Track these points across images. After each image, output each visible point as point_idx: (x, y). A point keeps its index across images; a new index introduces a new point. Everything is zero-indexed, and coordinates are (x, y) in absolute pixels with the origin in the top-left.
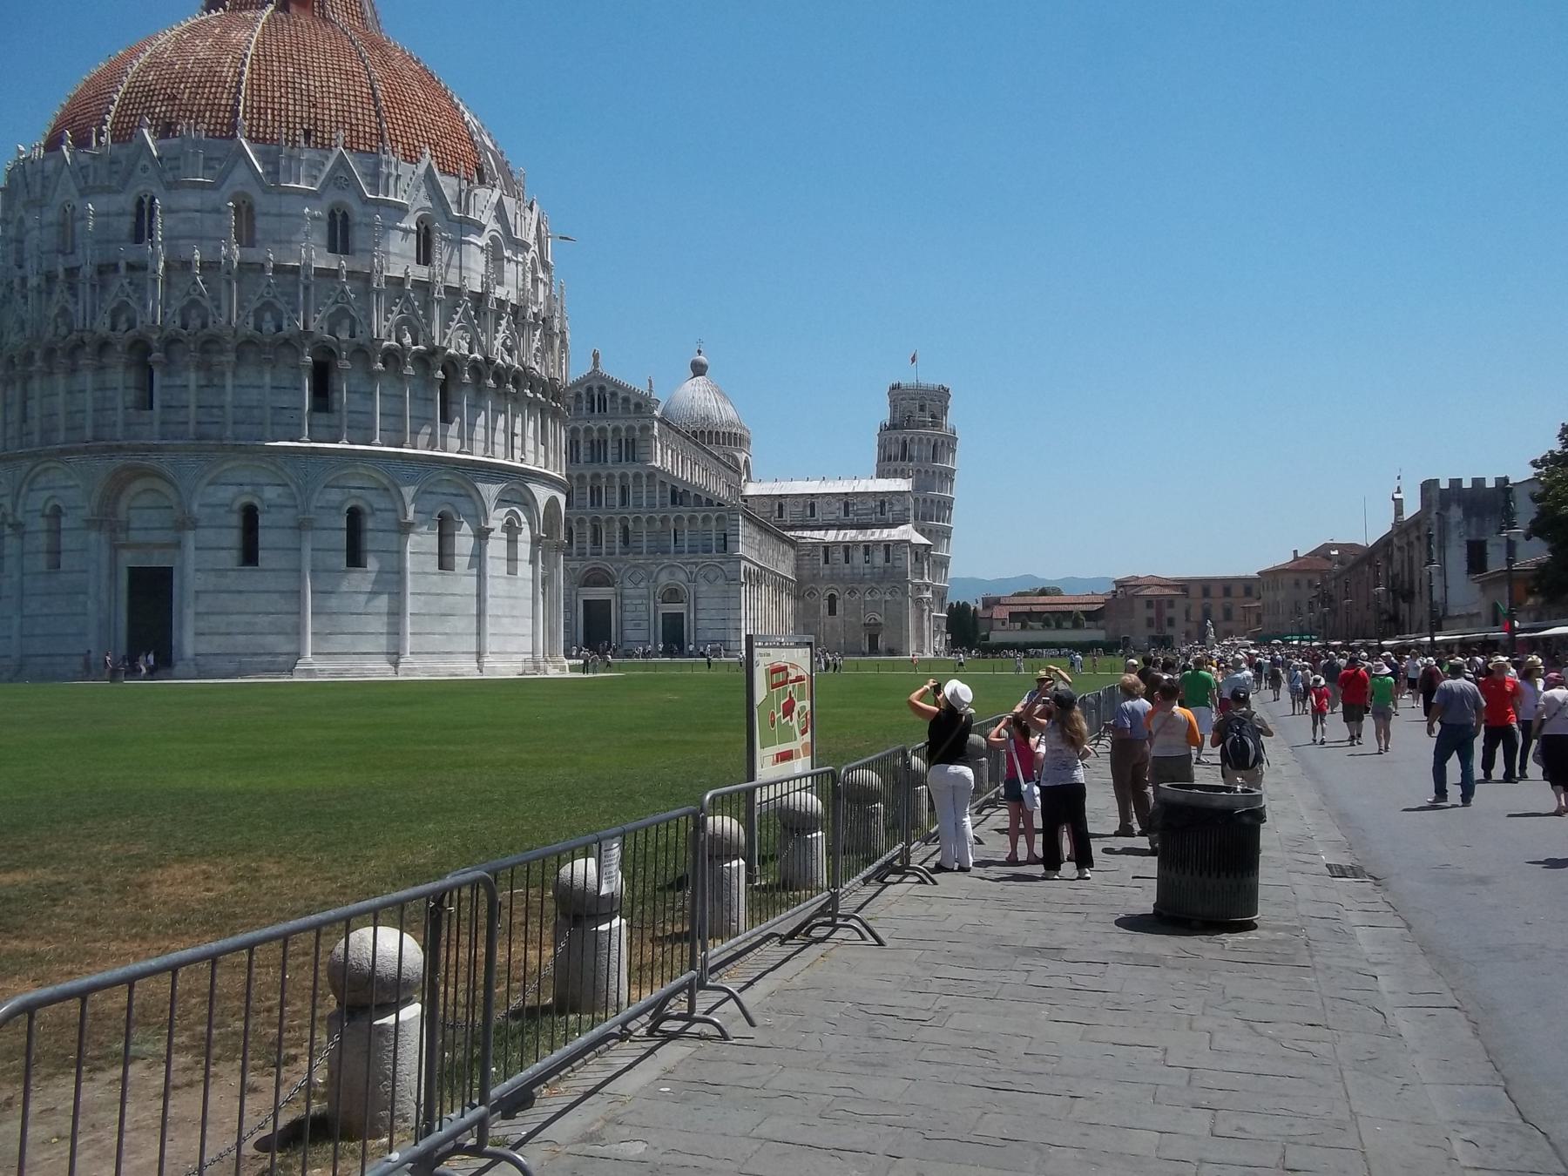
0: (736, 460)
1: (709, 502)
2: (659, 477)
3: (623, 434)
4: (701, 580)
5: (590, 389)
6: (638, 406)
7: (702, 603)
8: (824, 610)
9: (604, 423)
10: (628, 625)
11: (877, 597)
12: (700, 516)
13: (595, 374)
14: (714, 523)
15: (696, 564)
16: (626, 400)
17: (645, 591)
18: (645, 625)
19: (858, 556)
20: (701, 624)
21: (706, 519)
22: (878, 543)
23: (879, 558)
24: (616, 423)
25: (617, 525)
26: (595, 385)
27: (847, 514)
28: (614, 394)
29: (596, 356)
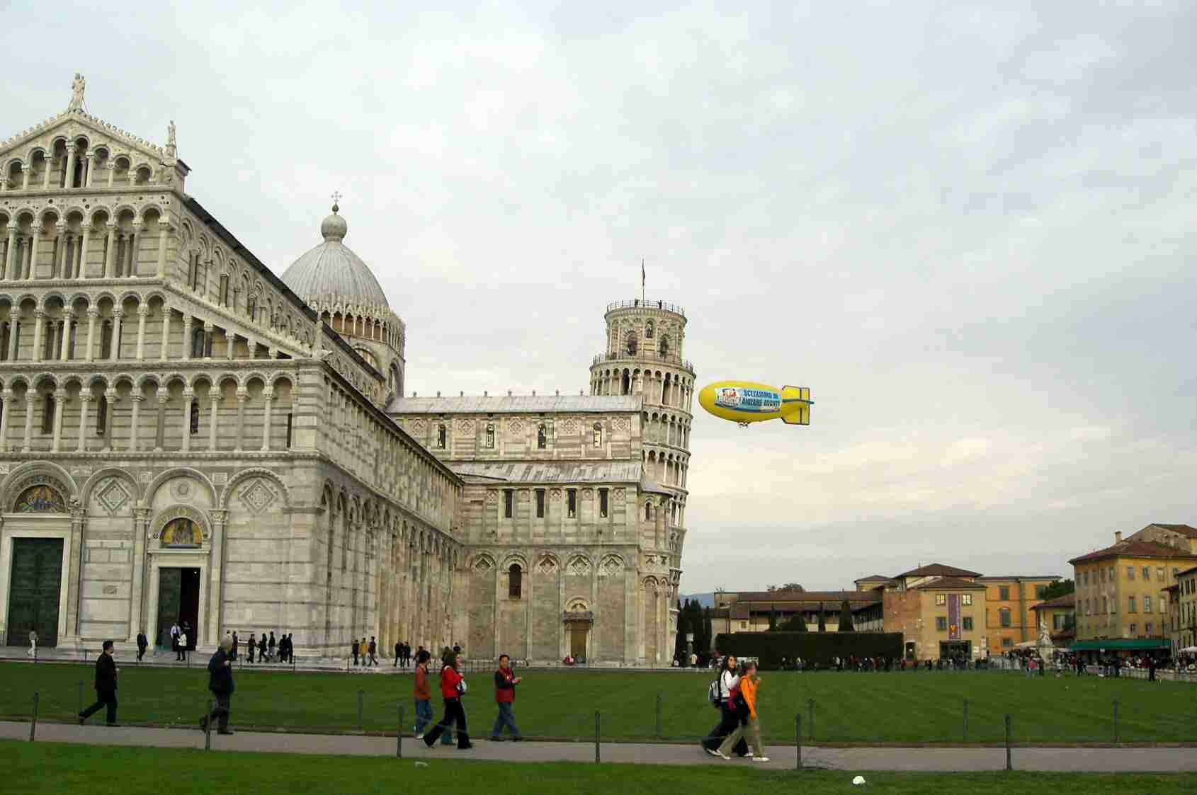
0: (376, 360)
1: (262, 350)
2: (170, 303)
3: (112, 221)
4: (235, 504)
5: (60, 145)
6: (144, 172)
7: (239, 550)
8: (502, 591)
9: (78, 203)
10: (91, 589)
11: (586, 571)
12: (242, 377)
13: (76, 115)
14: (268, 390)
15: (230, 471)
16: (123, 163)
17: (128, 525)
18: (123, 590)
19: (556, 504)
20: (232, 592)
21: (255, 383)
22: (588, 486)
23: (589, 508)
24: (103, 202)
25: (86, 391)
26: (70, 134)
27: (542, 441)
28: (102, 153)
29: (79, 84)
